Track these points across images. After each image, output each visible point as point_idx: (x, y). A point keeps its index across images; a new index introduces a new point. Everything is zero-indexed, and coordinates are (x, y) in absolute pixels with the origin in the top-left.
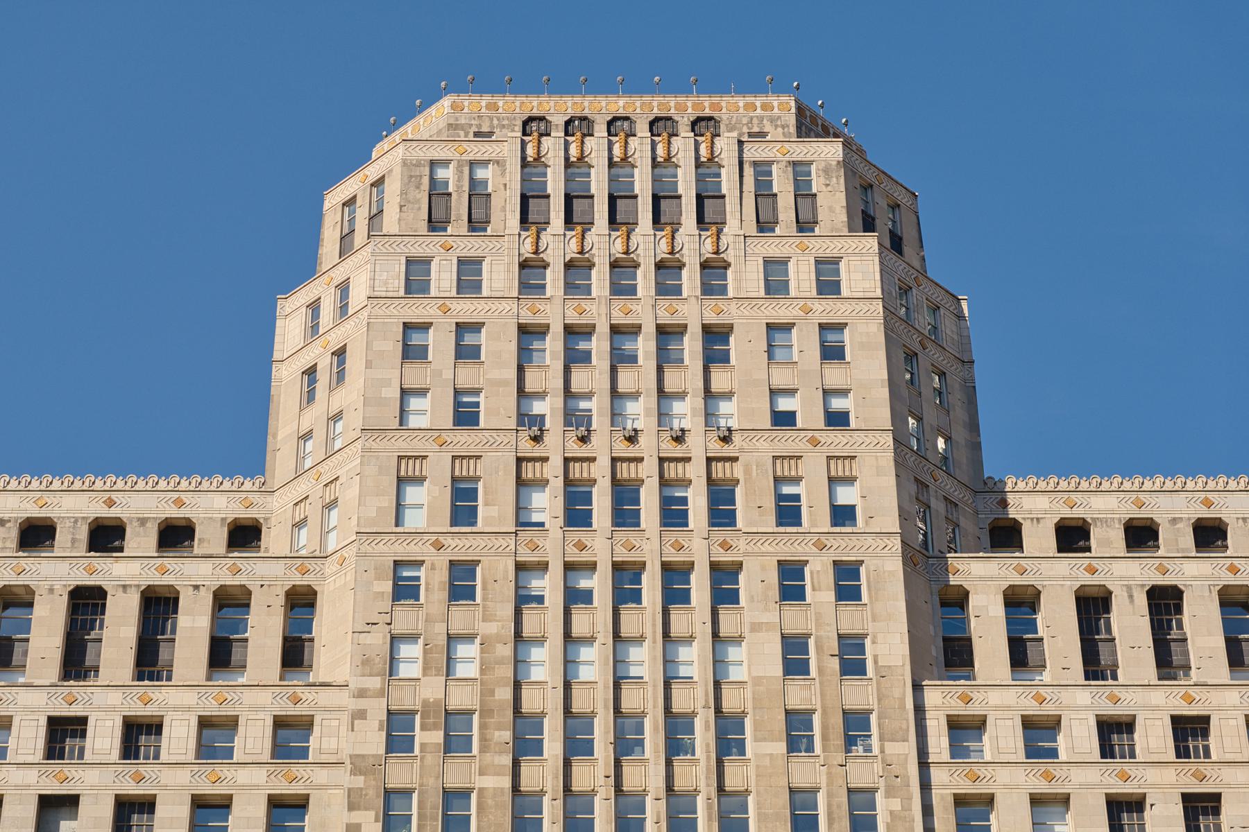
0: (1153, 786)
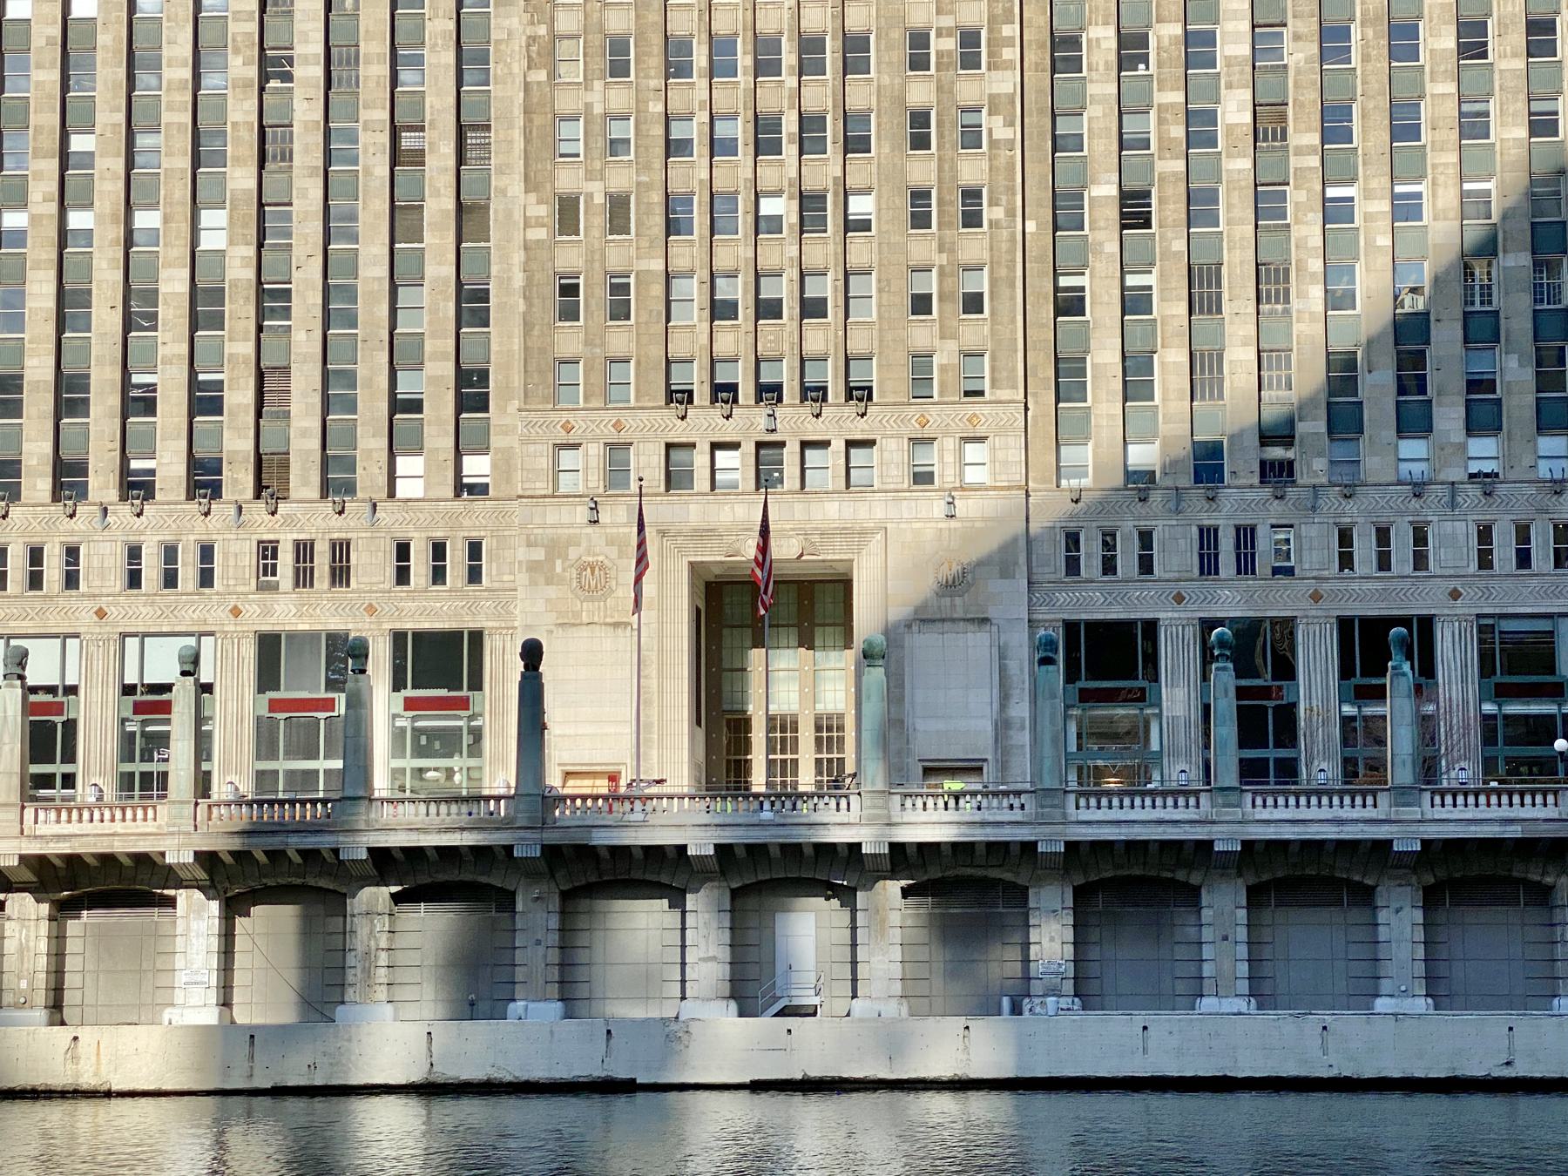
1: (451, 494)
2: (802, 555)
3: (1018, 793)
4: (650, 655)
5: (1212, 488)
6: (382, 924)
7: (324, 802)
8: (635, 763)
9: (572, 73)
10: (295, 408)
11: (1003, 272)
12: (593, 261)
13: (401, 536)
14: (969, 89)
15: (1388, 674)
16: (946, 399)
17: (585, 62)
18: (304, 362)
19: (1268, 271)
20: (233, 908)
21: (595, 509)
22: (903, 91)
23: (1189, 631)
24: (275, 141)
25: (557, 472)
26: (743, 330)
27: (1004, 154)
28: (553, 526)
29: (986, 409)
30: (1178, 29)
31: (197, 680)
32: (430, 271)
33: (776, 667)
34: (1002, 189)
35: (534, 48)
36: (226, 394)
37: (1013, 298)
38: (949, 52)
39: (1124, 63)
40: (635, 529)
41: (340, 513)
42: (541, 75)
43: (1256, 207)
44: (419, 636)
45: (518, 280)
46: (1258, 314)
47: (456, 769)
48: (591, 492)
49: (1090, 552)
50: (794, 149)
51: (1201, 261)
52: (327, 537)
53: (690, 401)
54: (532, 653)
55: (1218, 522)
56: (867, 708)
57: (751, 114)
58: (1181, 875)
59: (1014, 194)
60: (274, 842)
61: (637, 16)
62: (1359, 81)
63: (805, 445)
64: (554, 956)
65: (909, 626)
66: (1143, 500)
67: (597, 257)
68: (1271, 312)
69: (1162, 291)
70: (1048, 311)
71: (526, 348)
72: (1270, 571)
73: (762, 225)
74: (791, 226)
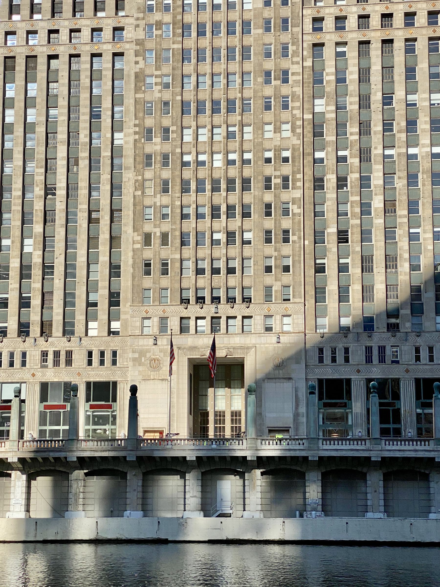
0: (373, 37)
1: (106, 334)
2: (227, 356)
3: (302, 439)
4: (174, 390)
5: (370, 333)
6: (81, 483)
7: (62, 441)
8: (168, 428)
9: (150, 192)
10: (55, 306)
11: (297, 258)
12: (156, 255)
13: (90, 349)
14: (285, 196)
15: (433, 399)
16: (277, 302)
17: (154, 188)
18: (58, 290)
19: (389, 257)
20: (31, 478)
21: (156, 340)
22: (262, 196)
24: (49, 216)
25: (143, 327)
26: (207, 278)
27: (297, 218)
29: (291, 305)
30: (357, 175)
31: (20, 399)
32: (101, 259)
33: (218, 394)
34: (296, 230)
35: (137, 184)
36: (32, 301)
37: (300, 267)
38: (278, 184)
39: (339, 187)
40: (170, 347)
41: (69, 341)
42: (139, 193)
43: (385, 236)
44: (95, 383)
45: (131, 261)
46: (386, 272)
47: (107, 429)
48: (154, 334)
49: (327, 355)
50: (225, 217)
51: (366, 254)
52: (65, 349)
53: (189, 303)
54: (134, 390)
55: (373, 345)
56: (249, 409)
57: (210, 205)
58: (359, 469)
59: (301, 231)
60: (45, 455)
61: (172, 173)
62: (421, 193)
63: (228, 318)
64: (140, 495)
65: (264, 380)
66: (346, 337)
67: (157, 253)
68: (391, 272)
69: (352, 265)
70: (312, 271)
71: (133, 285)
72: (390, 362)
73: (214, 242)
74: (224, 243)
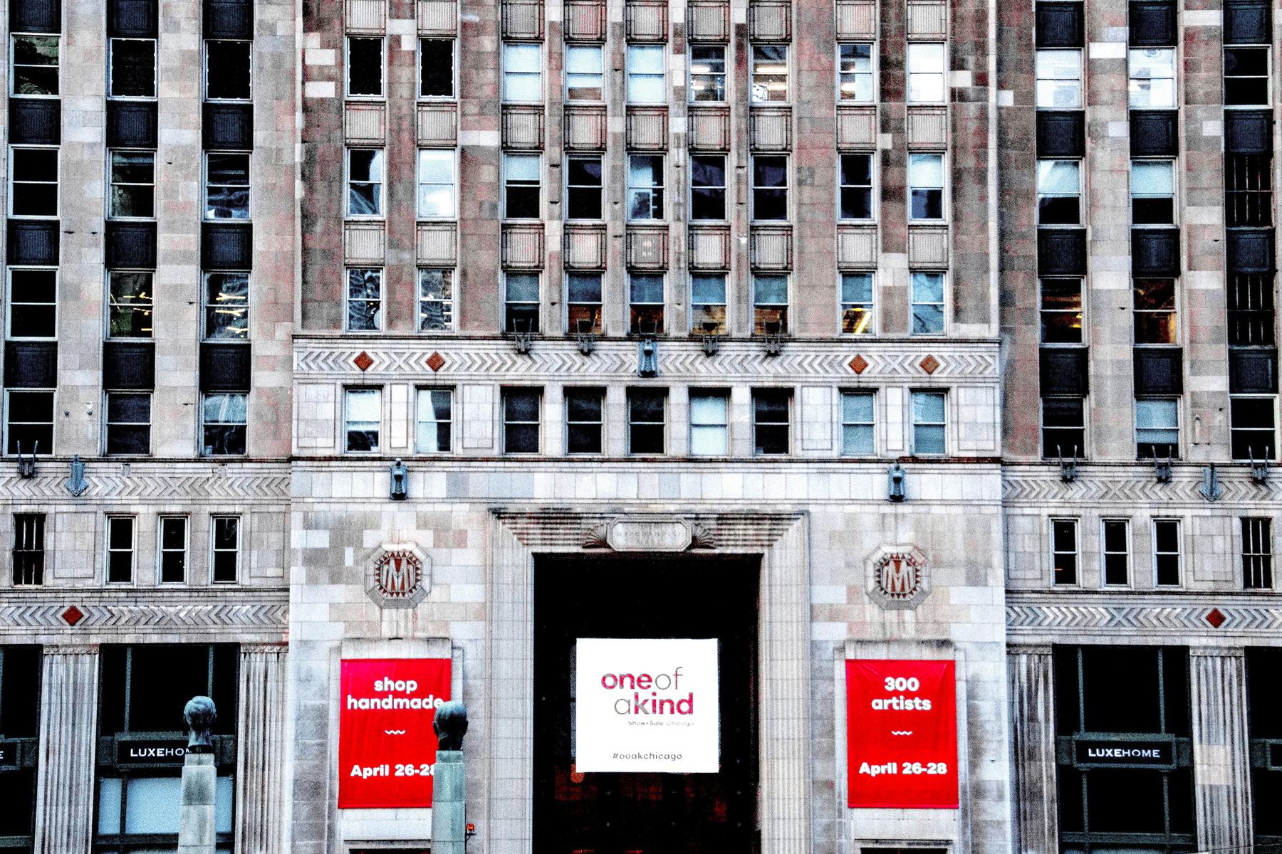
12: (399, 131)
23: (1231, 666)
28: (340, 501)
37: (983, 198)
44: (141, 650)
52: (10, 510)
55: (1269, 514)
66: (1164, 480)
67: (406, 124)
71: (305, 250)
